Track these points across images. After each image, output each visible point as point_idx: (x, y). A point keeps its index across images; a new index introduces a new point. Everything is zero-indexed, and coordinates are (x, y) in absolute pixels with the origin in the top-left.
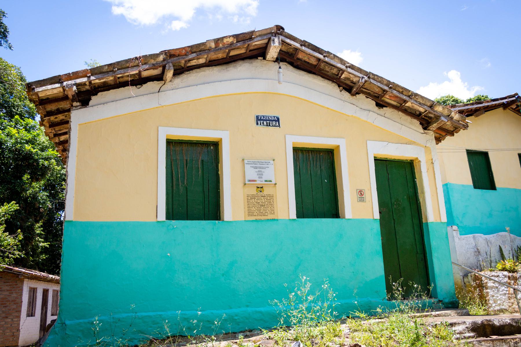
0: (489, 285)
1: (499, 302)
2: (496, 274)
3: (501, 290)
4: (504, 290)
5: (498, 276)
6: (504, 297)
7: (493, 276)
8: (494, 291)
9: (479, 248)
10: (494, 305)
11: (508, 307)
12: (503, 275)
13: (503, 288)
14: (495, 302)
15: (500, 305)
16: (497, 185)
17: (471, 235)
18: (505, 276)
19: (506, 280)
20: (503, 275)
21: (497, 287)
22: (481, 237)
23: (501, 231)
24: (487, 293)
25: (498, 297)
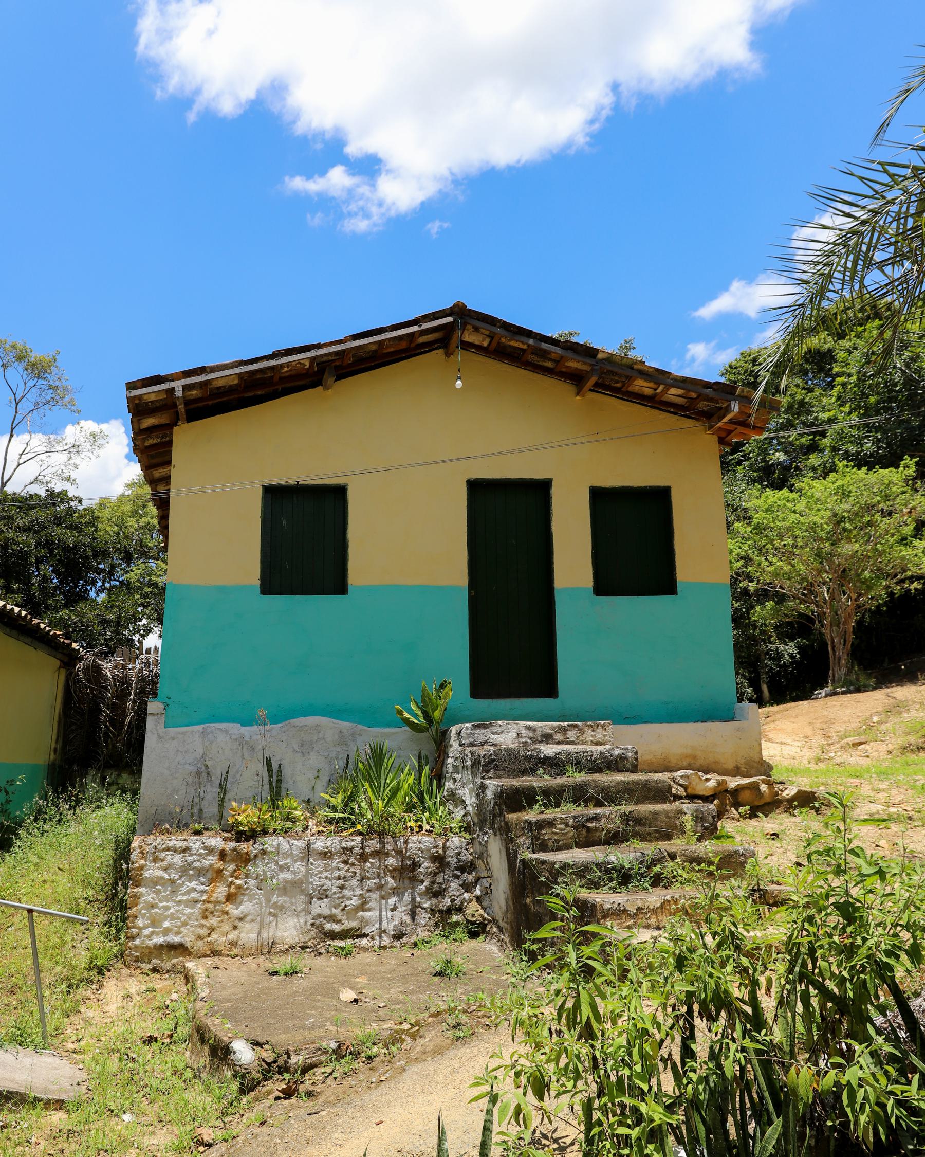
0: (146, 874)
1: (166, 924)
2: (179, 844)
3: (184, 889)
4: (195, 890)
5: (185, 850)
6: (188, 911)
7: (168, 849)
8: (158, 892)
9: (209, 763)
10: (146, 932)
11: (193, 938)
12: (205, 848)
13: (193, 884)
14: (154, 923)
15: (166, 932)
16: (354, 577)
17: (200, 728)
18: (211, 851)
19: (212, 860)
20: (205, 848)
21: (173, 882)
22: (227, 732)
23: (305, 714)
24: (136, 896)
25: (167, 908)
